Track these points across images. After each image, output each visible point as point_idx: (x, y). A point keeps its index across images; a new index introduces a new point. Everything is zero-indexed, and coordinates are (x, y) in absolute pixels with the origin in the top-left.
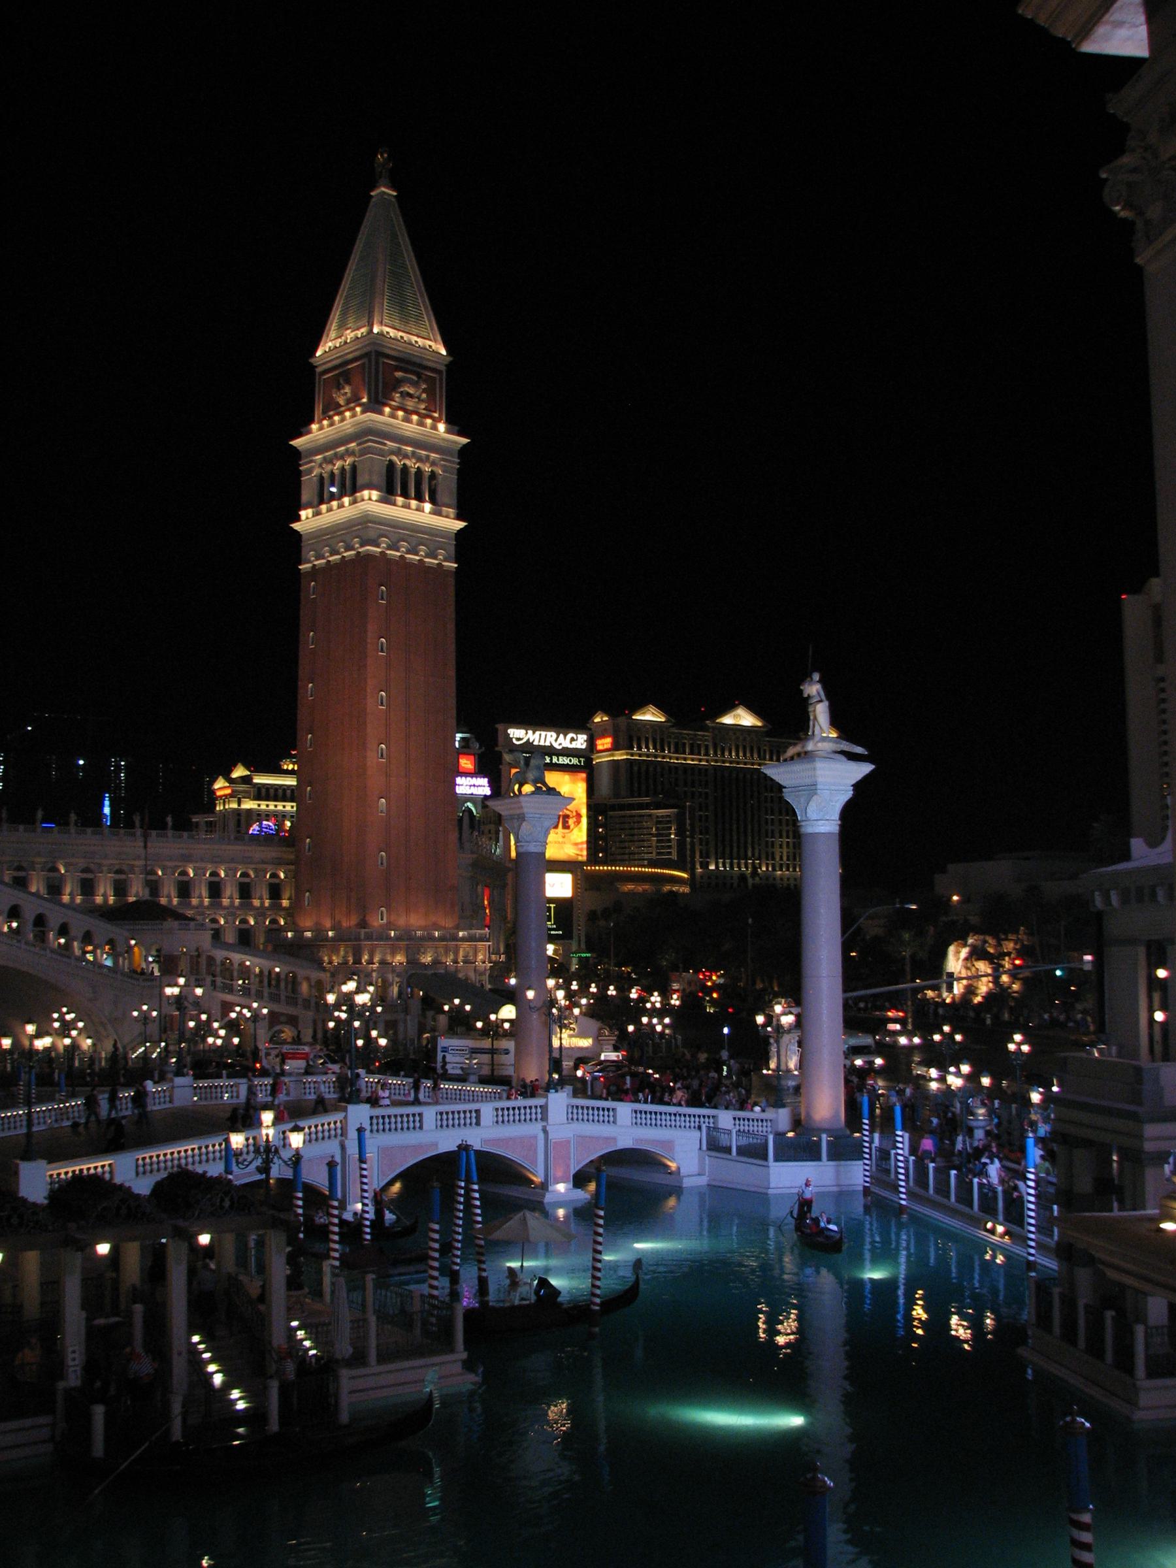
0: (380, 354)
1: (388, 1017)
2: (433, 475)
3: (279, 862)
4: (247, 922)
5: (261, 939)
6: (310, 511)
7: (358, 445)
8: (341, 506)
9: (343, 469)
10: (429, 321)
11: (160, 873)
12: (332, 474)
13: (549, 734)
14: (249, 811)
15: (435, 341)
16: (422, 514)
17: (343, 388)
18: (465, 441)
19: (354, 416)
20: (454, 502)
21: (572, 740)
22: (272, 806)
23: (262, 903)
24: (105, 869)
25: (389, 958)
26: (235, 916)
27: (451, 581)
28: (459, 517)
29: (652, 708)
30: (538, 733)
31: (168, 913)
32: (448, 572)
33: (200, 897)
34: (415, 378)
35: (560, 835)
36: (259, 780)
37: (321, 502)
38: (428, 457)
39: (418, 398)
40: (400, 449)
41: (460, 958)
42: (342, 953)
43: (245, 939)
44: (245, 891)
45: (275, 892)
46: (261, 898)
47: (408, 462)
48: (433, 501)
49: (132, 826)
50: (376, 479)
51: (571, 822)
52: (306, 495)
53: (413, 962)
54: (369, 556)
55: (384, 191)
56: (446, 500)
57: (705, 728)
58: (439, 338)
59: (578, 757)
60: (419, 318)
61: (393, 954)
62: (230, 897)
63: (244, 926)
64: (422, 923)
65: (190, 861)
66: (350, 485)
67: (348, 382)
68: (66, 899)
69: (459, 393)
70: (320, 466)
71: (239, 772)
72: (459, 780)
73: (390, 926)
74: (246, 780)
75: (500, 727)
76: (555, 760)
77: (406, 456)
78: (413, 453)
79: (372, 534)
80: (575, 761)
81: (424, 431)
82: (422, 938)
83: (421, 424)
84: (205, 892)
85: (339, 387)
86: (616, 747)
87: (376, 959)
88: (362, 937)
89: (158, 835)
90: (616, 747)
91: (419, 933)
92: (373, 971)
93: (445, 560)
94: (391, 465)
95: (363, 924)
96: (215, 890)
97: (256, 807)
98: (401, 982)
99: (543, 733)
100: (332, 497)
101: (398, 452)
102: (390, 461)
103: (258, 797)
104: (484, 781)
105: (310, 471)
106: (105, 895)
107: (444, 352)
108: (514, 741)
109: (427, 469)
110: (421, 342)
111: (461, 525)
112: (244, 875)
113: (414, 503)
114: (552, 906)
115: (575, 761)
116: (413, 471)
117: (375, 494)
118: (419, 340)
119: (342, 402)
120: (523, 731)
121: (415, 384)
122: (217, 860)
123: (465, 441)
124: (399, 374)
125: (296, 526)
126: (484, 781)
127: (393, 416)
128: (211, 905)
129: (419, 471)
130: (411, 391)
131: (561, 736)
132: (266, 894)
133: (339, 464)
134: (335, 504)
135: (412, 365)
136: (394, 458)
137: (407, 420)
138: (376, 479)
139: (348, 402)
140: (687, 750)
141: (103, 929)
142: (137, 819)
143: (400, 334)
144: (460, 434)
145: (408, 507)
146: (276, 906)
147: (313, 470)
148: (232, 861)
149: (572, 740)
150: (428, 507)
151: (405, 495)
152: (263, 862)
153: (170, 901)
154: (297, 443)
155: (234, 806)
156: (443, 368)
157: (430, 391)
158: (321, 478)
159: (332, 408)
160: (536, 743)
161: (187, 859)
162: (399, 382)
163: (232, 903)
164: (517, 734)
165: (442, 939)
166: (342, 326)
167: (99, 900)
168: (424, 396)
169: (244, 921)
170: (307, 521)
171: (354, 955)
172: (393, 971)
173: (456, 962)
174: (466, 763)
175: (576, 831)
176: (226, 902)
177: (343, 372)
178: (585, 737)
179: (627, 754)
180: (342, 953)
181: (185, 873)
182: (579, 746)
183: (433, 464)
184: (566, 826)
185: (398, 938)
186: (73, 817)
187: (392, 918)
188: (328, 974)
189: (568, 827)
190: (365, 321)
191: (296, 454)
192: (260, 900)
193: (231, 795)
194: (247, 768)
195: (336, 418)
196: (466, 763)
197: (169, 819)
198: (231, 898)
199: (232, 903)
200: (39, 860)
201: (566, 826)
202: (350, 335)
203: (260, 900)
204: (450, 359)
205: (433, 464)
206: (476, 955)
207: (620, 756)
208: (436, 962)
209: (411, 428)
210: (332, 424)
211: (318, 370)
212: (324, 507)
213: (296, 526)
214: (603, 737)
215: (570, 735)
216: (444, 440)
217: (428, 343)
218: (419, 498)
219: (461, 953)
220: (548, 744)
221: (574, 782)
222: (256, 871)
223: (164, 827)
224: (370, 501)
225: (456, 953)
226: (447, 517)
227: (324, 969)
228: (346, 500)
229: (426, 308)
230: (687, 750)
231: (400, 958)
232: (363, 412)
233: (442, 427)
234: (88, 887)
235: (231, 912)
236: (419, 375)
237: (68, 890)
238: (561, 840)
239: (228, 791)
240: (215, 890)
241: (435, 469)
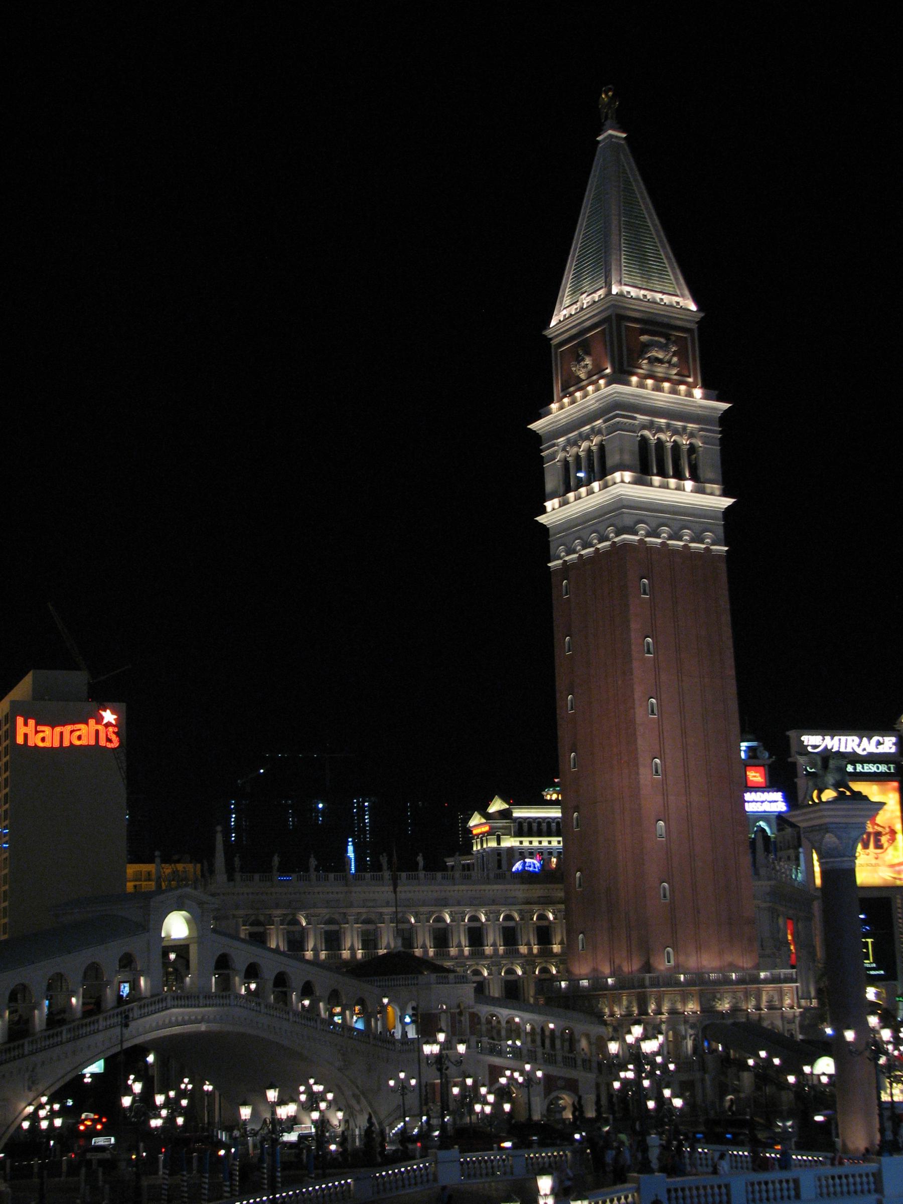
0: (621, 318)
1: (684, 1077)
2: (692, 449)
3: (547, 902)
4: (513, 972)
5: (531, 992)
6: (556, 501)
7: (605, 422)
8: (590, 492)
9: (589, 451)
10: (674, 276)
11: (413, 920)
12: (578, 457)
13: (850, 738)
14: (511, 850)
15: (683, 296)
16: (682, 494)
17: (583, 360)
18: (725, 406)
19: (597, 389)
20: (720, 478)
21: (879, 743)
22: (535, 842)
23: (530, 950)
24: (351, 918)
25: (679, 1007)
26: (499, 966)
27: (723, 567)
28: (725, 494)
30: (836, 738)
31: (424, 964)
32: (719, 556)
33: (459, 945)
34: (663, 340)
35: (872, 856)
36: (519, 813)
37: (568, 490)
38: (685, 428)
39: (669, 362)
40: (652, 422)
41: (764, 1004)
42: (625, 1003)
43: (513, 993)
44: (510, 937)
45: (544, 935)
46: (528, 944)
47: (662, 436)
48: (694, 477)
49: (379, 868)
50: (627, 459)
51: (884, 839)
52: (551, 483)
53: (708, 1010)
54: (626, 545)
55: (612, 134)
56: (710, 475)
58: (687, 292)
60: (662, 272)
61: (685, 1003)
62: (493, 944)
63: (511, 977)
64: (715, 963)
65: (446, 905)
66: (599, 467)
67: (588, 353)
68: (309, 955)
69: (714, 353)
70: (564, 449)
71: (497, 805)
72: (748, 796)
73: (678, 969)
74: (505, 814)
75: (792, 734)
76: (859, 768)
77: (660, 430)
78: (668, 426)
79: (628, 521)
80: (883, 768)
81: (677, 399)
82: (716, 982)
83: (674, 391)
84: (464, 941)
85: (579, 360)
87: (665, 1008)
88: (647, 982)
89: (408, 878)
91: (713, 976)
92: (662, 1022)
93: (713, 544)
94: (644, 440)
95: (647, 967)
96: (476, 936)
97: (518, 844)
98: (697, 1035)
99: (843, 738)
100: (580, 483)
101: (650, 426)
102: (642, 436)
103: (520, 833)
105: (553, 457)
106: (352, 949)
107: (693, 307)
109: (685, 441)
110: (667, 299)
111: (727, 502)
112: (508, 918)
113: (673, 482)
114: (869, 940)
115: (883, 768)
116: (669, 445)
117: (628, 476)
118: (664, 297)
119: (583, 376)
120: (820, 738)
121: (663, 347)
122: (477, 902)
123: (725, 406)
124: (644, 338)
125: (542, 519)
126: (778, 796)
127: (641, 385)
128: (473, 955)
129: (676, 446)
130: (660, 355)
132: (533, 939)
133: (585, 445)
134: (583, 490)
135: (659, 325)
136: (646, 433)
137: (658, 389)
138: (627, 459)
139: (590, 375)
141: (350, 986)
142: (384, 860)
143: (643, 292)
144: (719, 399)
145: (666, 486)
146: (546, 953)
147: (557, 453)
148: (494, 902)
149: (879, 743)
150: (689, 485)
151: (662, 473)
152: (528, 902)
153: (426, 952)
154: (535, 426)
155: (493, 844)
156: (694, 326)
157: (682, 354)
158: (566, 463)
159: (572, 384)
161: (444, 903)
162: (646, 347)
163: (496, 951)
164: (812, 741)
165: (740, 981)
166: (577, 290)
167: (346, 954)
168: (675, 359)
169: (511, 972)
170: (554, 513)
171: (639, 1008)
172: (686, 1022)
173: (758, 1008)
174: (755, 776)
175: (890, 850)
176: (488, 950)
177: (581, 342)
178: (894, 739)
180: (625, 1003)
181: (440, 919)
183: (692, 435)
184: (879, 846)
185: (688, 983)
186: (313, 862)
187: (682, 959)
188: (610, 1029)
190: (602, 282)
191: (536, 439)
192: (528, 946)
193: (489, 833)
194: (505, 800)
195: (578, 394)
196: (755, 776)
197: (420, 859)
198: (494, 945)
199: (496, 951)
200: (278, 912)
201: (879, 846)
202: (585, 300)
203: (528, 946)
204: (702, 315)
205: (692, 435)
206: (781, 1000)
208: (735, 1010)
209: (663, 398)
210: (573, 402)
211: (554, 342)
212: (571, 495)
213: (542, 519)
215: (875, 739)
216: (700, 407)
217: (675, 299)
218: (679, 475)
219: (764, 998)
220: (849, 750)
222: (521, 912)
223: (414, 867)
224: (623, 485)
225: (758, 999)
226: (712, 494)
227: (605, 1023)
228: (596, 485)
229: (668, 258)
231: (692, 1007)
232: (608, 384)
233: (698, 393)
234: (333, 941)
235: (495, 962)
236: (667, 337)
237: (311, 945)
238: (874, 861)
239: (486, 829)
240: (476, 936)
241: (694, 441)
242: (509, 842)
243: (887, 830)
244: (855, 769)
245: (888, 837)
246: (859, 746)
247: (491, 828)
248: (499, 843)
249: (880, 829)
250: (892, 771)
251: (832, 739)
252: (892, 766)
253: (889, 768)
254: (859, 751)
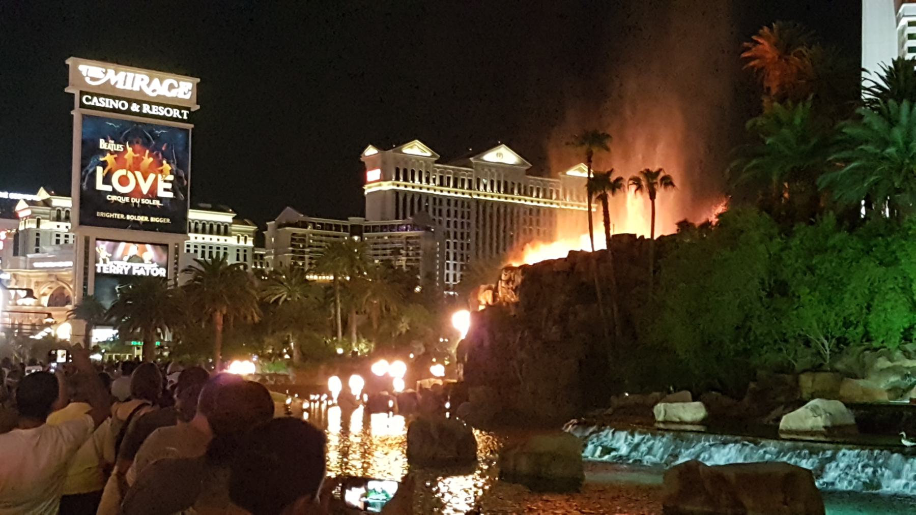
21: (171, 87)
29: (417, 143)
30: (122, 74)
57: (469, 165)
59: (180, 108)
74: (46, 203)
76: (146, 109)
86: (384, 178)
90: (384, 178)
99: (130, 75)
108: (88, 80)
131: (156, 81)
140: (451, 184)
149: (171, 87)
160: (120, 86)
179: (393, 184)
182: (181, 96)
193: (31, 217)
207: (387, 186)
214: (373, 168)
230: (451, 184)
239: (29, 212)
244: (141, 108)
246: (148, 85)
247: (33, 212)
248: (38, 226)
250: (185, 117)
251: (116, 74)
252: (185, 112)
253: (181, 114)
254: (148, 91)
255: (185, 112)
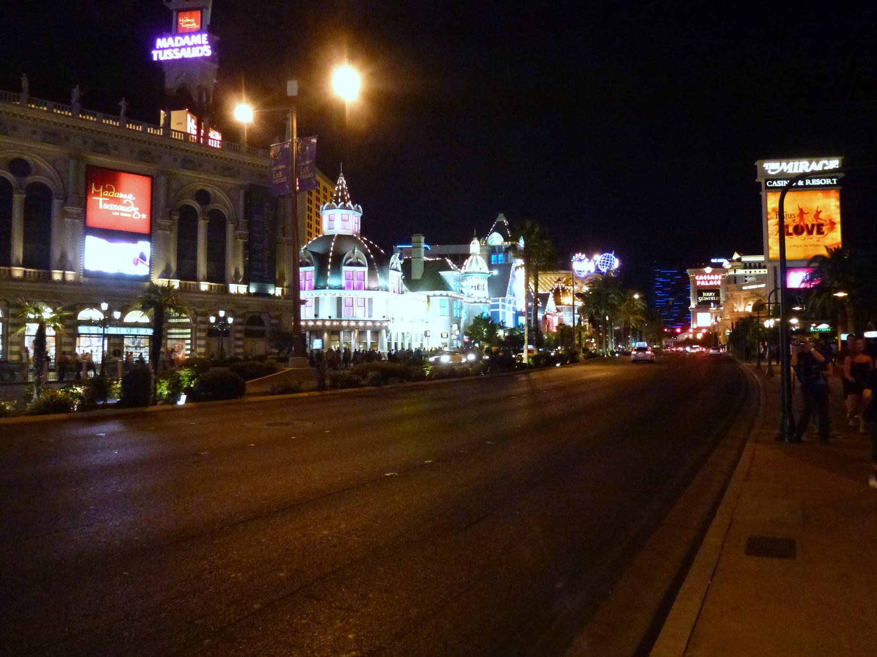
22: (753, 271)
30: (791, 164)
51: (824, 229)
71: (736, 256)
74: (739, 260)
76: (808, 182)
80: (828, 182)
99: (796, 163)
104: (203, 38)
115: (828, 182)
160: (790, 171)
164: (772, 167)
184: (820, 232)
189: (823, 233)
194: (739, 253)
201: (820, 232)
221: (828, 197)
238: (816, 243)
242: (740, 272)
243: (828, 222)
244: (805, 183)
245: (829, 226)
249: (821, 222)
252: (835, 180)
255: (835, 180)
